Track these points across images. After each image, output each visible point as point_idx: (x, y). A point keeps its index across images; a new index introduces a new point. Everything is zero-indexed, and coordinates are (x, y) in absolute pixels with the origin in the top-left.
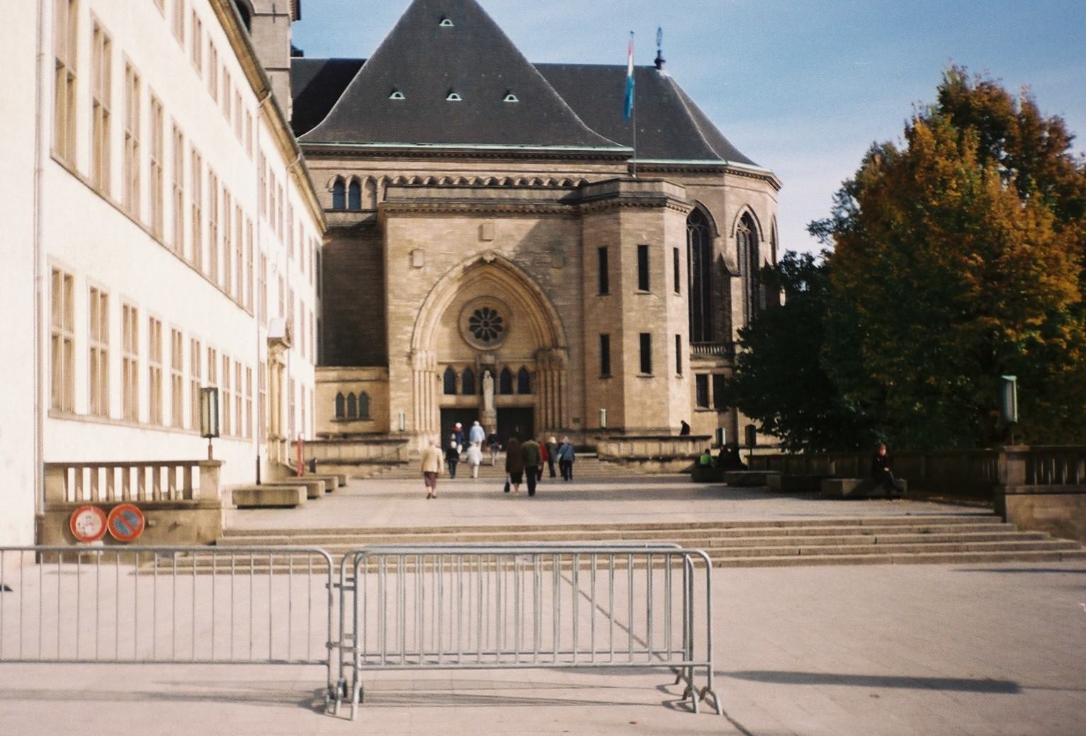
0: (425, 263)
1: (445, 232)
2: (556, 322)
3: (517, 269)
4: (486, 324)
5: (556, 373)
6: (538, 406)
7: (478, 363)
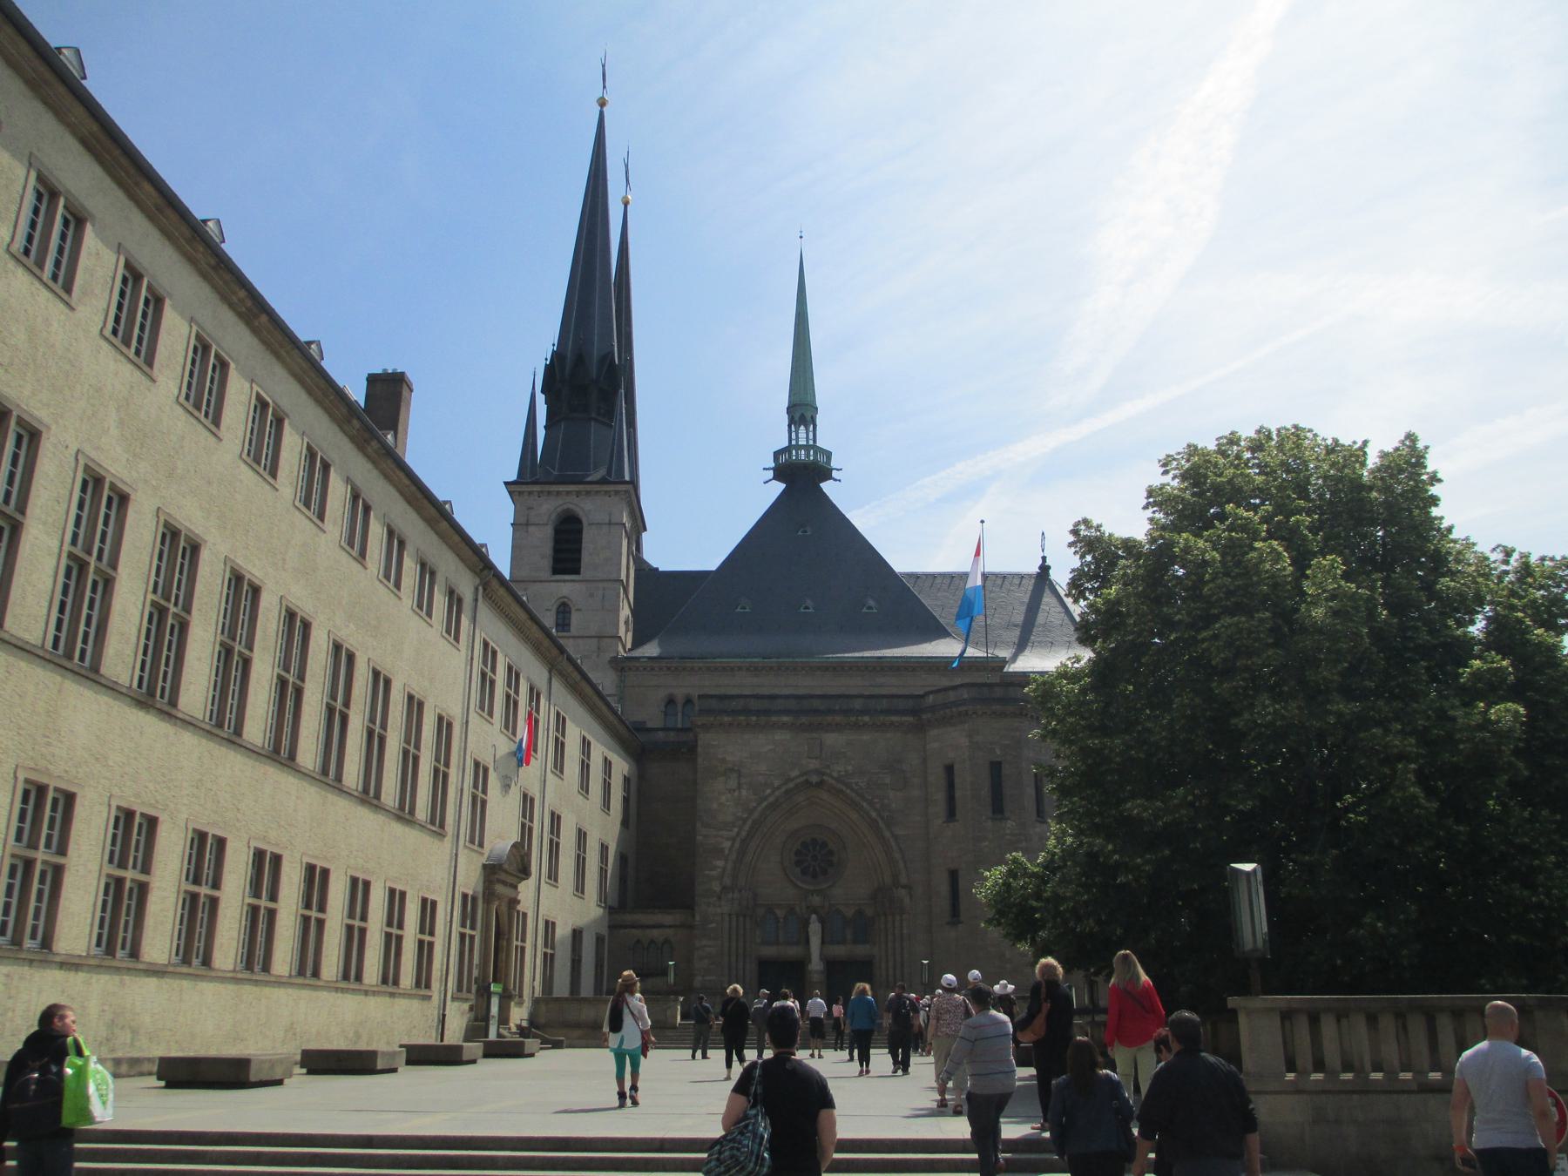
0: (739, 784)
2: (897, 856)
3: (848, 791)
5: (898, 918)
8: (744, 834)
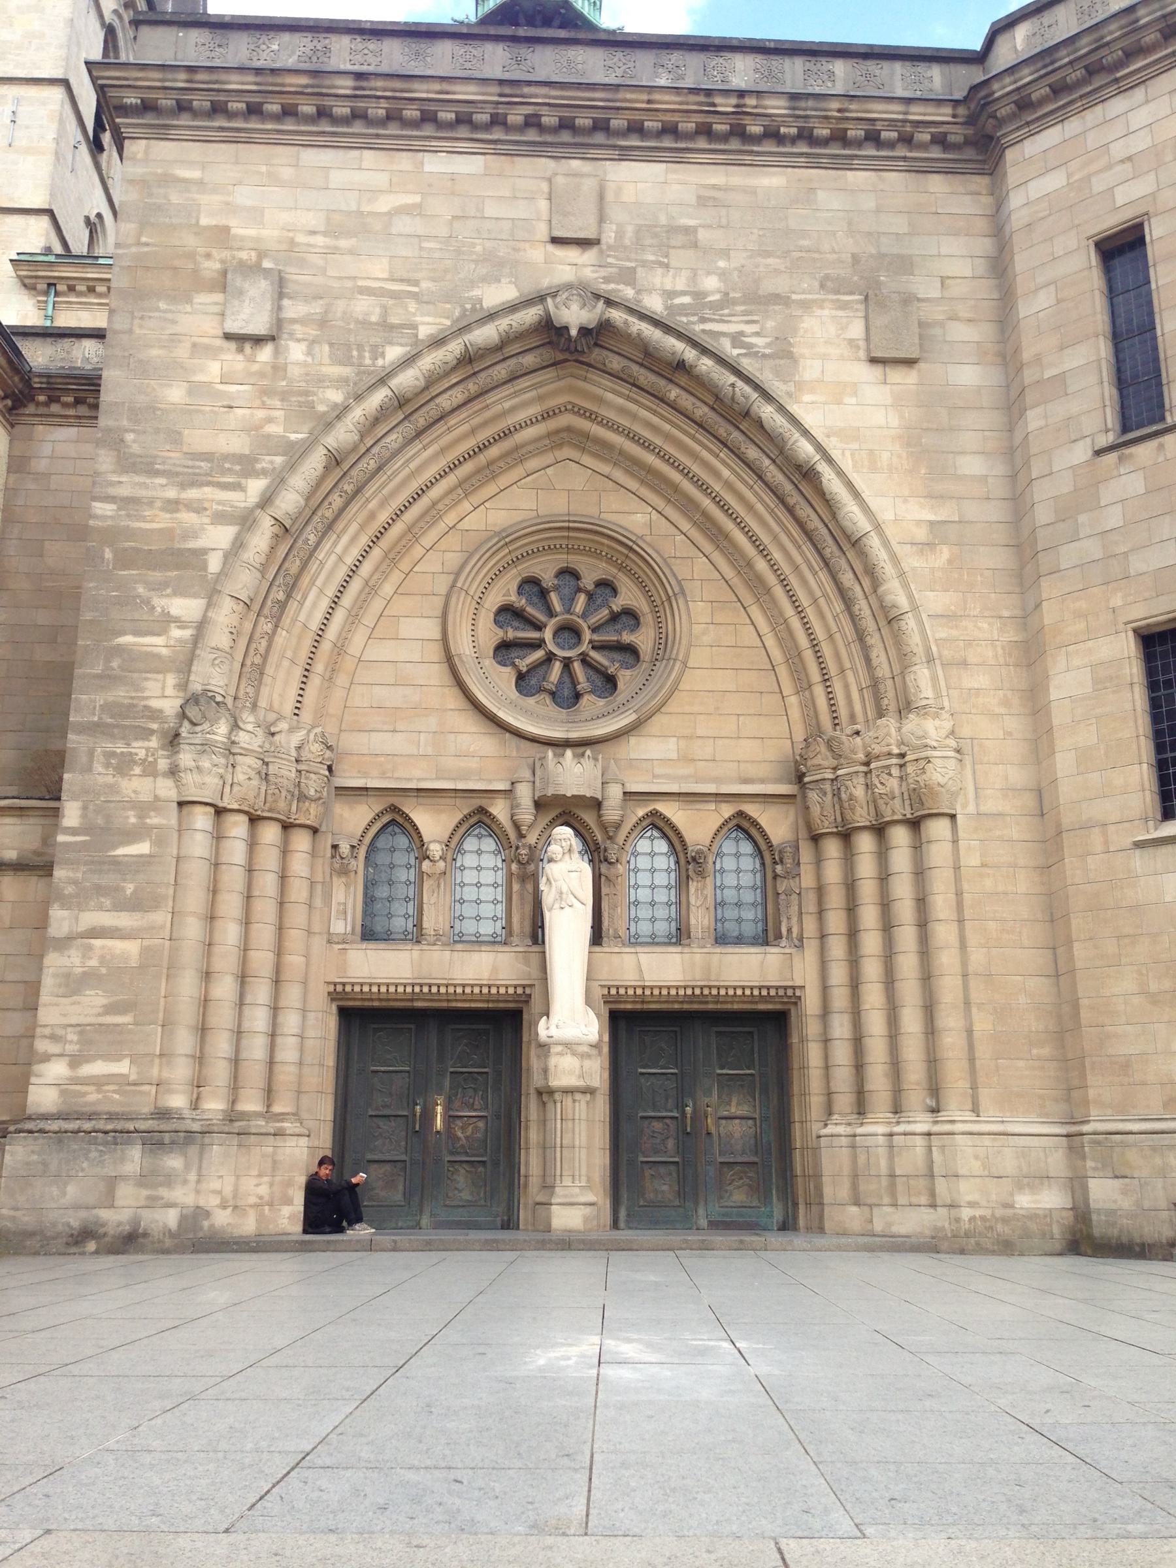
0: (279, 323)
1: (384, 204)
4: (569, 631)
6: (811, 1002)
7: (525, 794)
8: (289, 502)
